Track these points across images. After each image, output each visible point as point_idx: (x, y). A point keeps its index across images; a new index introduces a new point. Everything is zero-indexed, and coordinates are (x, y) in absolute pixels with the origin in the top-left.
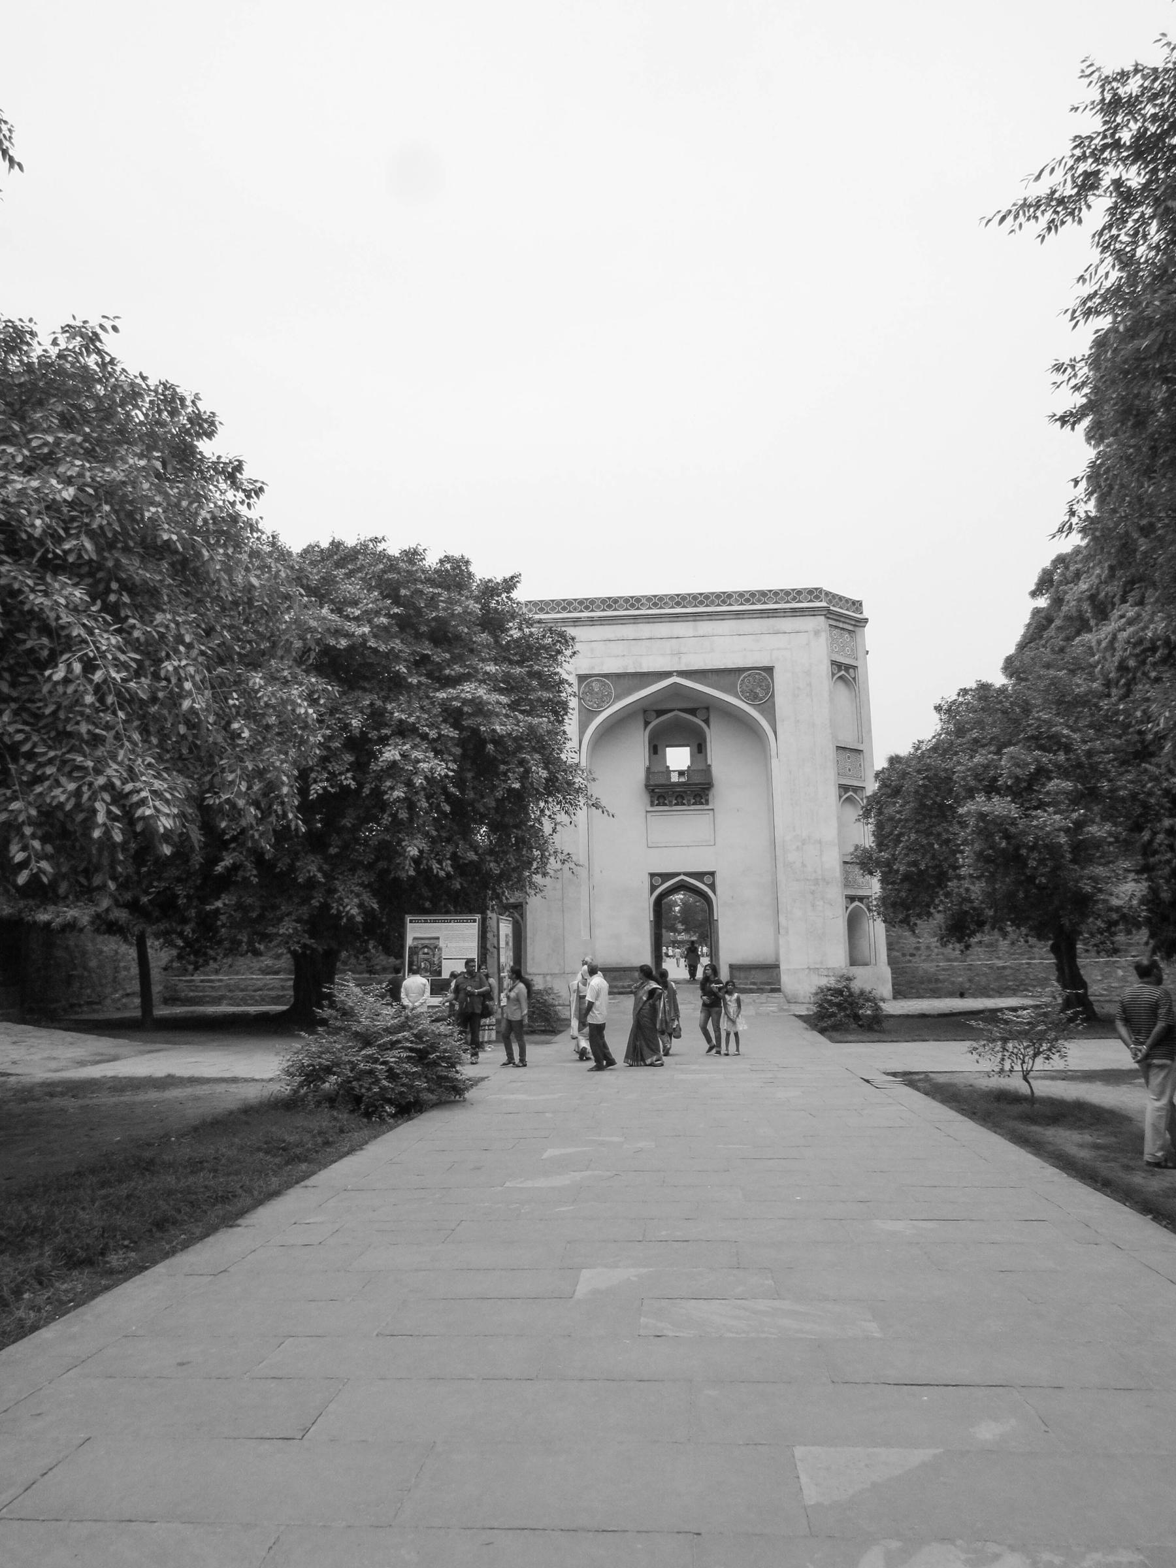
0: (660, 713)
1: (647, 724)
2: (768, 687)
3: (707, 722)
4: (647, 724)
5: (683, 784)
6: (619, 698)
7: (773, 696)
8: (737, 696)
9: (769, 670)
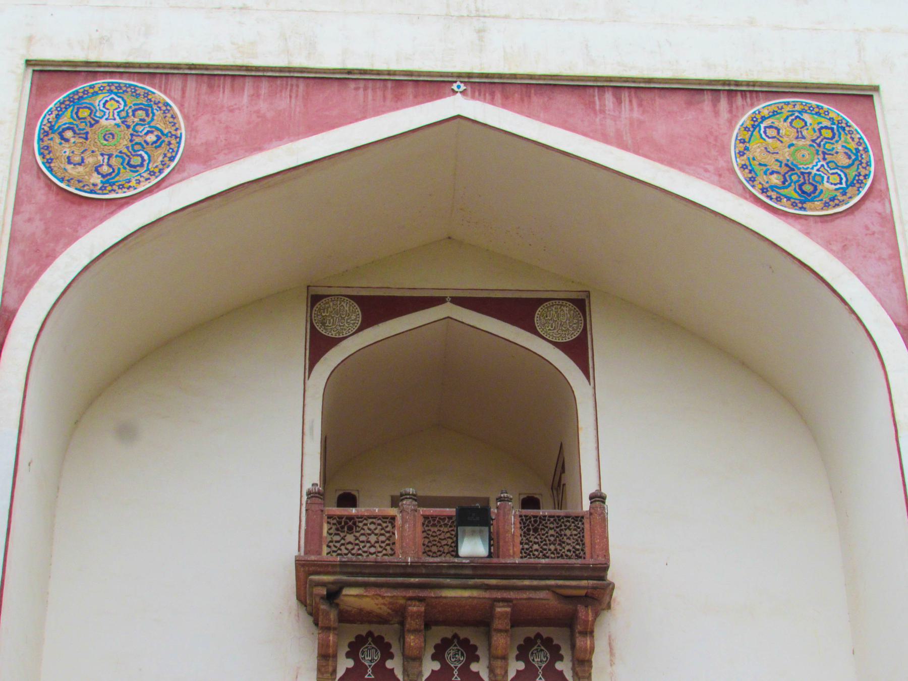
0: (377, 308)
1: (319, 345)
2: (857, 157)
3: (579, 351)
4: (319, 345)
5: (477, 569)
6: (205, 158)
7: (878, 192)
8: (723, 178)
9: (861, 98)
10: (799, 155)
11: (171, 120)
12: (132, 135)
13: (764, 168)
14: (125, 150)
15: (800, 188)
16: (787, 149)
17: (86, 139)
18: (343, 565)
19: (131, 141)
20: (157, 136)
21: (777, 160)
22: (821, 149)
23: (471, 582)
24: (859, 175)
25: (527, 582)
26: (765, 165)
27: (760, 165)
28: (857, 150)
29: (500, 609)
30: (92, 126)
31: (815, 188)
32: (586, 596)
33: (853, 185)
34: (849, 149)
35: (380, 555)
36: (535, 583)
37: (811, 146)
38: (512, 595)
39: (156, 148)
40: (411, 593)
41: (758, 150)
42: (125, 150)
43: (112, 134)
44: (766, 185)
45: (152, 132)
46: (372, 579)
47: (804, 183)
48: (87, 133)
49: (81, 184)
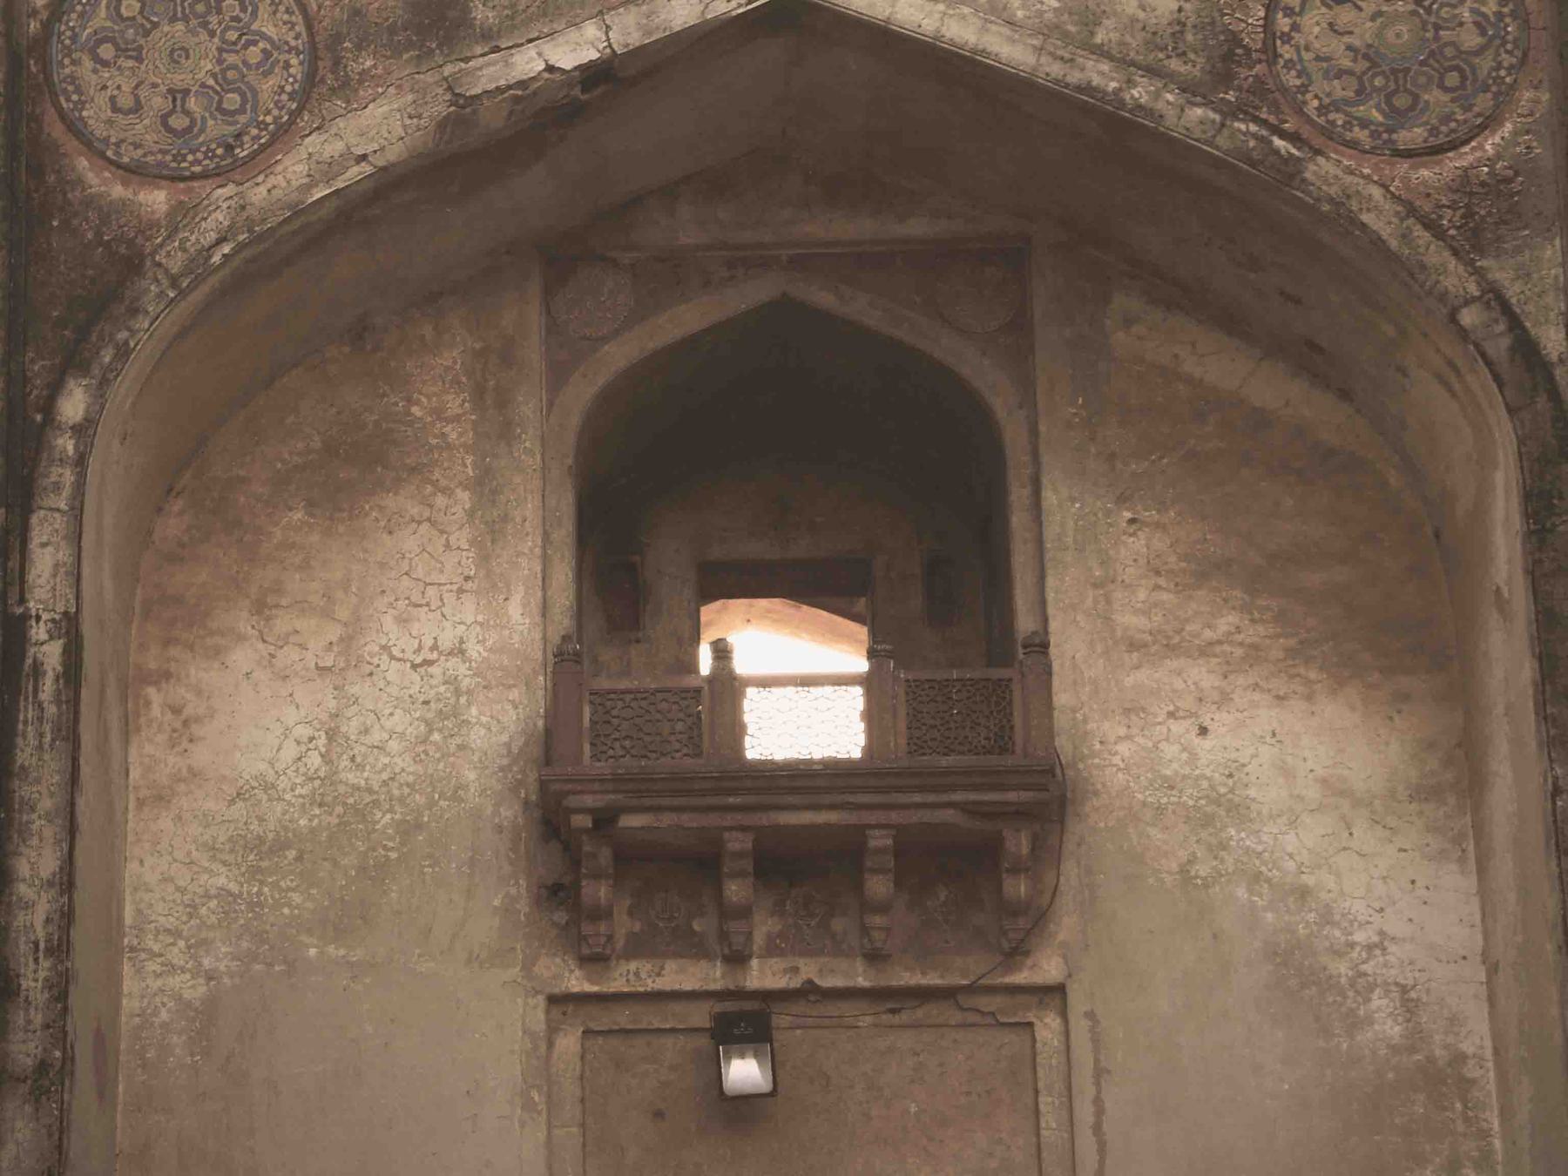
10: (1390, 34)
11: (286, 17)
12: (220, 50)
13: (1325, 65)
14: (211, 82)
15: (1389, 97)
16: (1369, 24)
17: (139, 59)
18: (617, 779)
19: (220, 61)
20: (264, 51)
21: (1349, 48)
22: (1433, 19)
23: (827, 799)
24: (1499, 66)
25: (917, 798)
26: (1328, 59)
27: (1318, 58)
28: (1500, 16)
29: (872, 843)
30: (147, 33)
31: (1416, 98)
32: (1017, 812)
33: (1486, 89)
34: (1484, 15)
35: (678, 755)
36: (931, 798)
37: (1414, 13)
38: (895, 817)
39: (266, 74)
40: (730, 819)
41: (1316, 30)
42: (211, 82)
43: (182, 48)
44: (1327, 101)
45: (255, 43)
46: (666, 802)
47: (1396, 91)
48: (141, 48)
49: (140, 152)
